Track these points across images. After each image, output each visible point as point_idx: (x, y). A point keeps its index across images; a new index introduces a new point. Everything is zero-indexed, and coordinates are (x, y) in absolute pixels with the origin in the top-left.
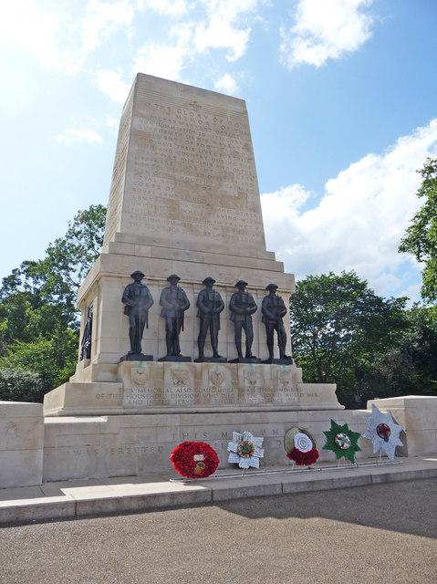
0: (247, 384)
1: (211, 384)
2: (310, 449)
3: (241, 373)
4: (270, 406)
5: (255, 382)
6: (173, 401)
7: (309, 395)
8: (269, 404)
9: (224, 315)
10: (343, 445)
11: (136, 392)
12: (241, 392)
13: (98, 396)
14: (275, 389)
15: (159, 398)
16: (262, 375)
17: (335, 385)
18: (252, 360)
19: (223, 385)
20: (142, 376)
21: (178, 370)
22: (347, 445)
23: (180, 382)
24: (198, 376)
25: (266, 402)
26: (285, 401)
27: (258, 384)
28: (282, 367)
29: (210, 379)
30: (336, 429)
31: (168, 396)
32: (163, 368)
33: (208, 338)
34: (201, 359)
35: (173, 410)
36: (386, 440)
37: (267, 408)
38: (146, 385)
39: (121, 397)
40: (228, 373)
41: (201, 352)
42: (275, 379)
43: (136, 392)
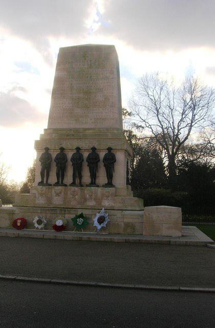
9: (85, 164)
23: (58, 195)
27: (93, 197)
33: (77, 175)
34: (73, 184)
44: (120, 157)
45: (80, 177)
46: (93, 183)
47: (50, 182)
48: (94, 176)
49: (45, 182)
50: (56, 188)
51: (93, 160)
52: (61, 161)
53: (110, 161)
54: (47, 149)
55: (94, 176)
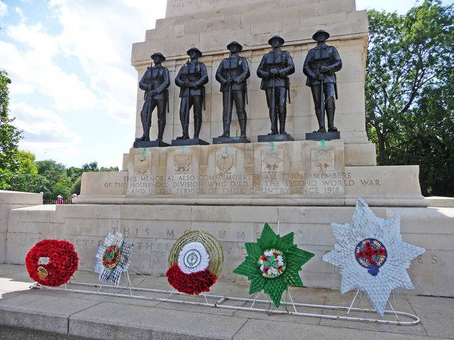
0: (264, 169)
1: (218, 171)
2: (202, 268)
3: (257, 155)
4: (297, 199)
5: (275, 166)
6: (174, 190)
7: (364, 183)
8: (296, 195)
9: (255, 82)
10: (266, 270)
11: (139, 180)
12: (257, 179)
13: (107, 185)
14: (307, 175)
15: (161, 188)
16: (288, 156)
17: (417, 167)
18: (281, 137)
19: (233, 170)
20: (144, 163)
21: (179, 155)
22: (273, 272)
23: (181, 169)
24: (203, 161)
25: (292, 193)
26: (322, 191)
28: (319, 143)
29: (217, 164)
30: (268, 240)
31: (170, 184)
32: (166, 154)
33: (235, 117)
35: (170, 200)
36: (374, 271)
37: (290, 201)
38: (148, 173)
39: (125, 185)
40: (241, 155)
41: (227, 132)
42: (307, 160)
43: (139, 180)
44: (353, 61)
45: (243, 121)
46: (278, 131)
47: (166, 139)
48: (278, 113)
49: (153, 136)
50: (178, 149)
51: (275, 73)
52: (193, 79)
53: (323, 67)
54: (158, 58)
55: (278, 113)
